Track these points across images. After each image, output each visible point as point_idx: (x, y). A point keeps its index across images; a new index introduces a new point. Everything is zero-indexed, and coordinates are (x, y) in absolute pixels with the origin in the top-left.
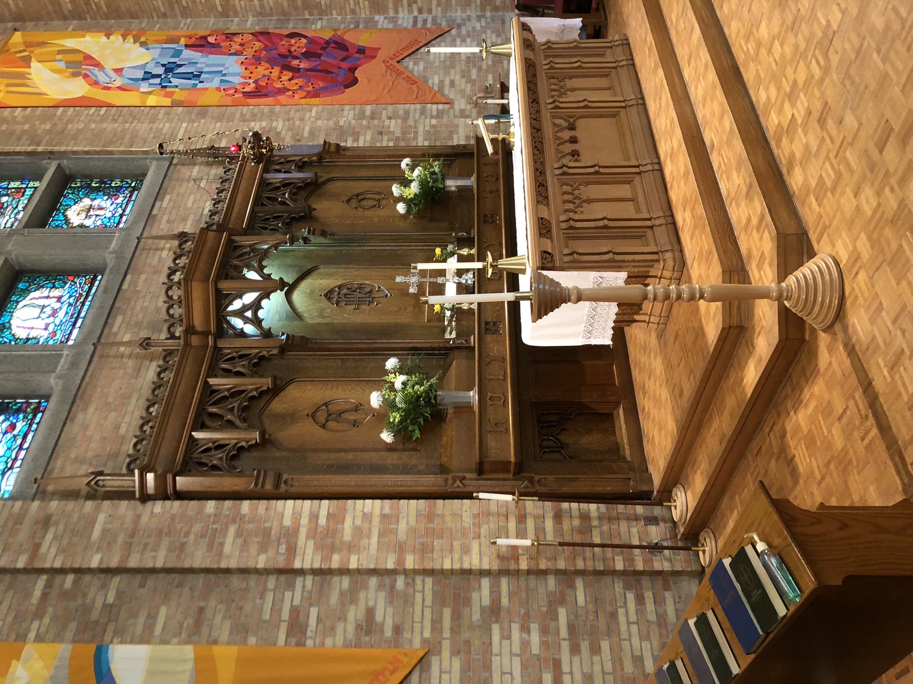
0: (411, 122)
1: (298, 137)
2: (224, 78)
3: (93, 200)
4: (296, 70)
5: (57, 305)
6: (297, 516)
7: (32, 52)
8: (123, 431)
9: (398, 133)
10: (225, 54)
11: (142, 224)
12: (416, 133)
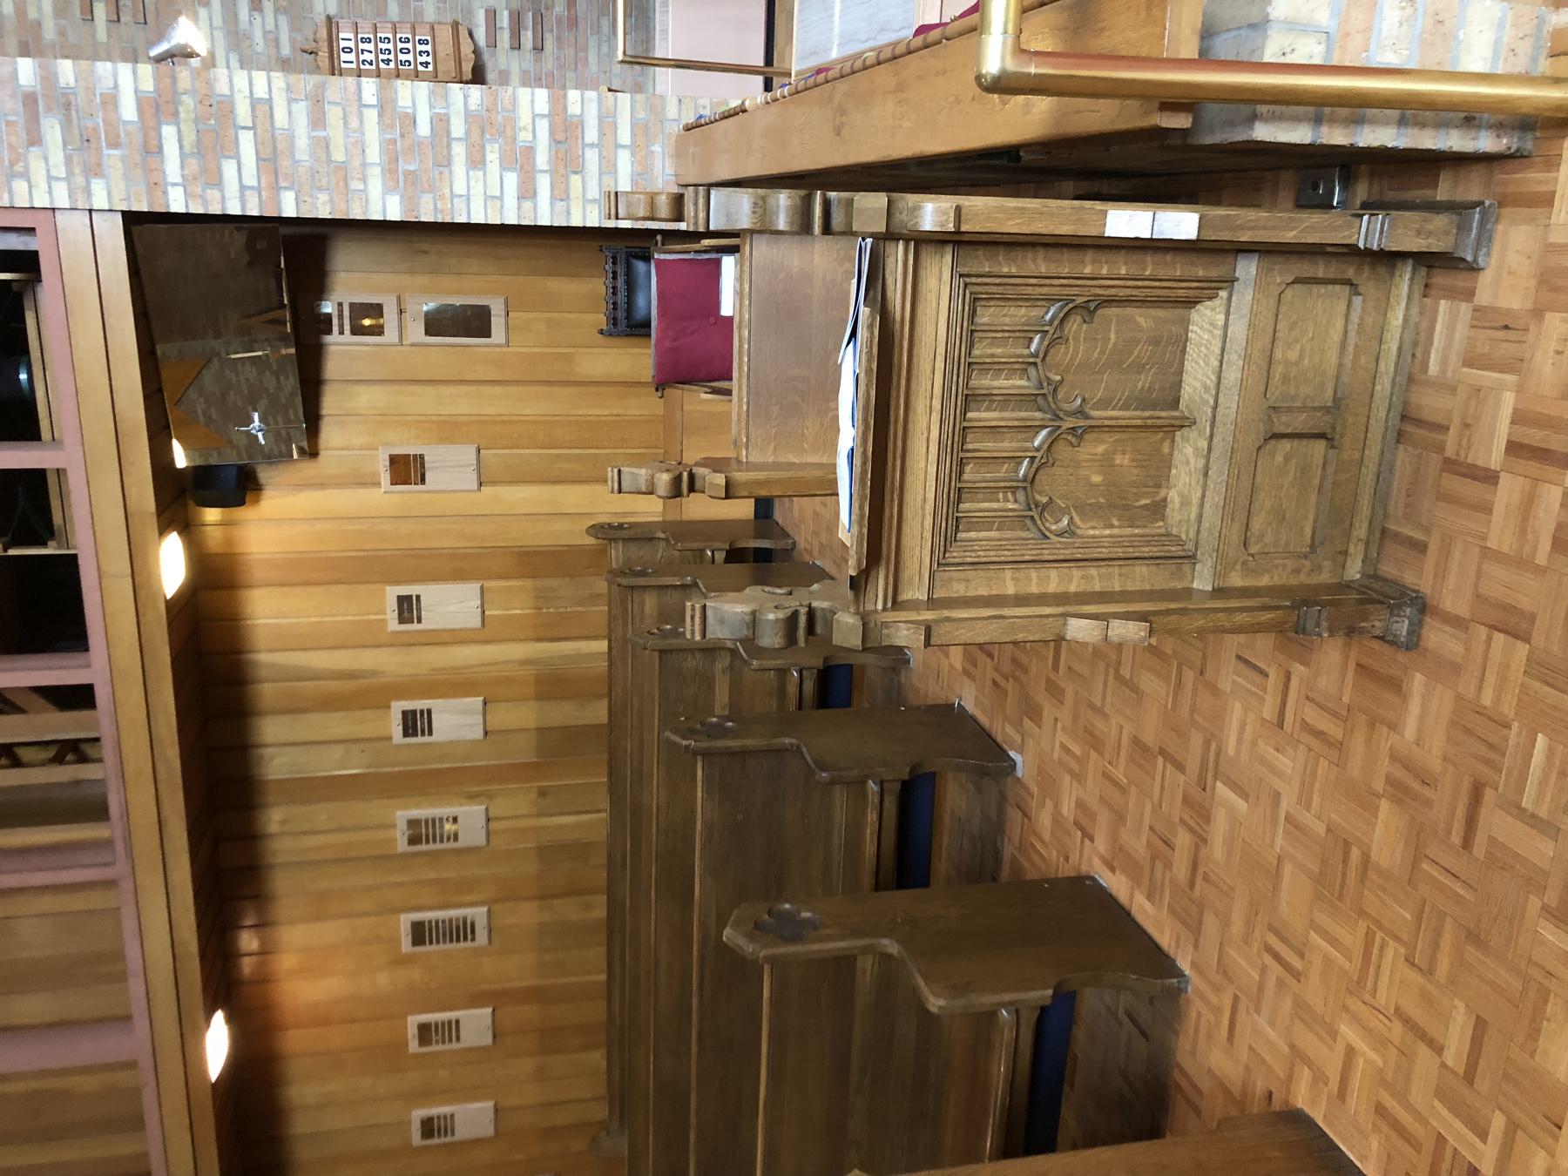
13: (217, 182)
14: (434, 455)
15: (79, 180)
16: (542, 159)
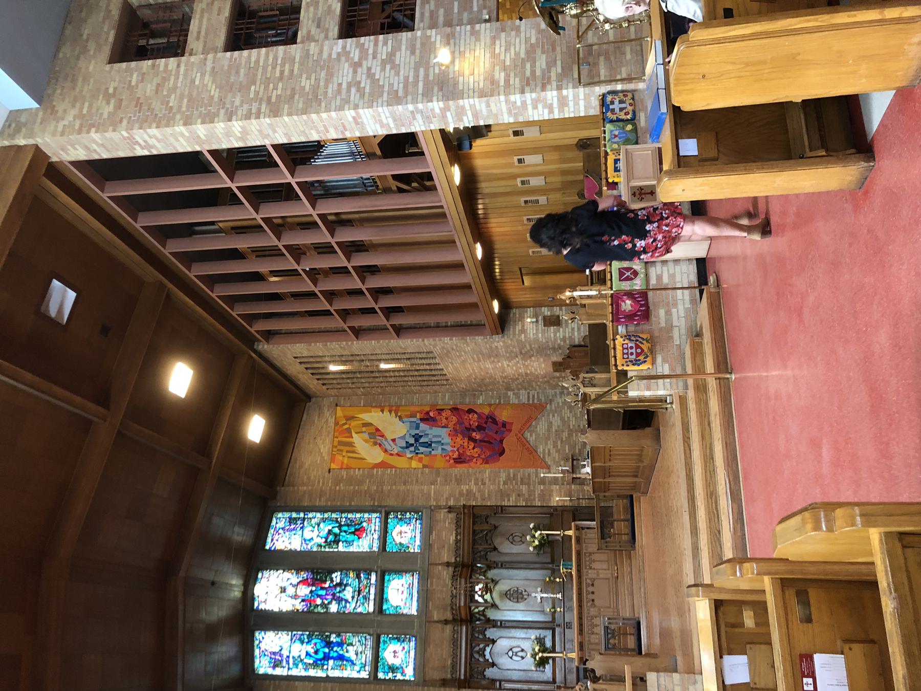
0: (532, 487)
2: (443, 447)
4: (474, 441)
7: (350, 425)
8: (444, 657)
9: (527, 496)
10: (439, 427)
12: (535, 495)
13: (462, 120)
14: (525, 130)
15: (427, 124)
16: (555, 105)
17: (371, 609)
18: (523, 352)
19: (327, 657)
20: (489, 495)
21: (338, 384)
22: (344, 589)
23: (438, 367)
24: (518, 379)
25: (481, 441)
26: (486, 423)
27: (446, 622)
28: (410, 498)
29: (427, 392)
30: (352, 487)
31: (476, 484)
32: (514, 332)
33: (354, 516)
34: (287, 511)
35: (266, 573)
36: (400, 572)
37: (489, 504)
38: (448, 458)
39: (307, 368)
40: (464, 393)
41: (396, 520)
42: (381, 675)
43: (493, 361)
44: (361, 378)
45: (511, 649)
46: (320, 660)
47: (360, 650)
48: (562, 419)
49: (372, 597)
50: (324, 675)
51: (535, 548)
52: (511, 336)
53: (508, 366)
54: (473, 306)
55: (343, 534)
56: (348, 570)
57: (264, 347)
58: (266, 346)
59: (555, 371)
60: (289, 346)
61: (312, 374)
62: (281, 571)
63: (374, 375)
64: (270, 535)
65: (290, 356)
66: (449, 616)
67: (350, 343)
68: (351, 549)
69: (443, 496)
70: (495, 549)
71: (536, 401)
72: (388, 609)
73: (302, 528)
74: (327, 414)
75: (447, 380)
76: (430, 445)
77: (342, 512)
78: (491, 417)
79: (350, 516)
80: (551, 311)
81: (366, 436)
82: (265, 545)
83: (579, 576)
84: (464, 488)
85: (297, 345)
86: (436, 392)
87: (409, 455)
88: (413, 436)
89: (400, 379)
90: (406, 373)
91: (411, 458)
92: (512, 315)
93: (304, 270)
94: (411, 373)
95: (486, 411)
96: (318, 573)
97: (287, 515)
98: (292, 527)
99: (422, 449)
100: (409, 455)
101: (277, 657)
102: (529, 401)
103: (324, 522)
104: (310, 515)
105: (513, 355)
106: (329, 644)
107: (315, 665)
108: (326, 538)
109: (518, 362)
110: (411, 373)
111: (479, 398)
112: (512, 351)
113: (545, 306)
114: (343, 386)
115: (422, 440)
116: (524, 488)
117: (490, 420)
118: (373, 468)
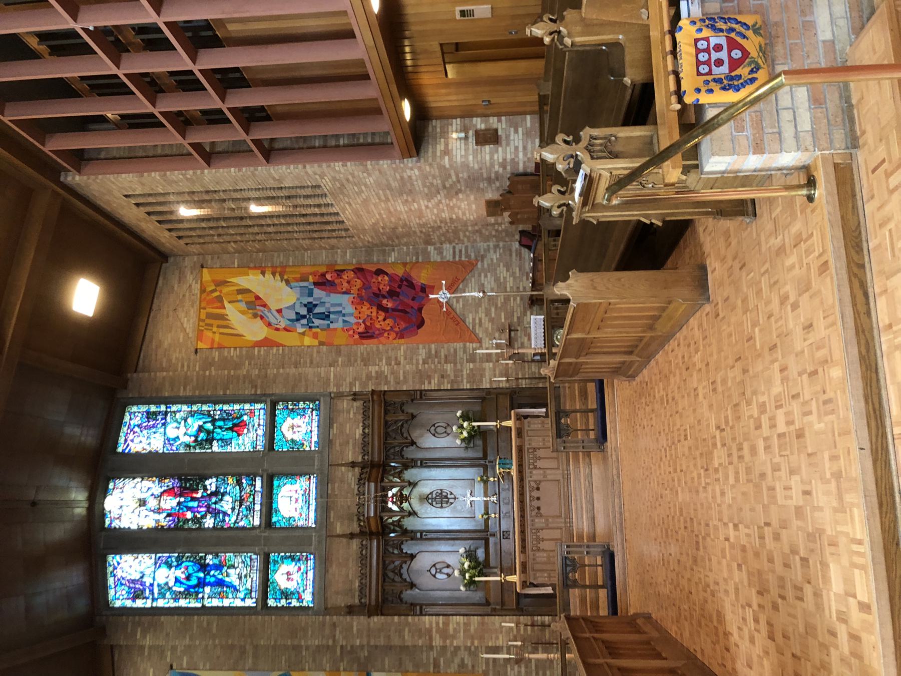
0: (459, 367)
1: (397, 380)
3: (293, 419)
4: (385, 310)
5: (296, 496)
6: (431, 623)
7: (221, 292)
9: (452, 378)
10: (340, 293)
11: (327, 449)
12: (462, 376)
17: (257, 522)
18: (448, 185)
19: (202, 583)
20: (405, 377)
21: (200, 236)
22: (221, 500)
23: (331, 210)
24: (440, 227)
25: (394, 310)
26: (400, 287)
27: (352, 536)
28: (303, 383)
29: (321, 248)
30: (226, 372)
31: (389, 364)
32: (434, 153)
33: (231, 408)
34: (143, 404)
35: (119, 483)
36: (293, 475)
37: (405, 389)
38: (351, 332)
39: (149, 214)
40: (369, 249)
41: (286, 412)
42: (271, 603)
43: (407, 201)
44: (228, 227)
45: (434, 565)
46: (194, 587)
47: (244, 572)
48: (497, 280)
49: (258, 507)
50: (199, 605)
51: (463, 440)
52: (430, 160)
53: (427, 207)
54: (371, 110)
55: (218, 430)
56: (225, 475)
57: (74, 179)
58: (77, 178)
59: (490, 214)
60: (111, 177)
61: (159, 222)
62: (139, 479)
63: (244, 223)
64: (121, 434)
65: (119, 195)
66: (356, 530)
67: (199, 172)
68: (229, 449)
69: (345, 380)
70: (413, 443)
71: (463, 258)
72: (278, 521)
73: (164, 424)
74: (190, 278)
75: (347, 230)
76: (328, 316)
77: (215, 403)
78: (407, 280)
79: (226, 407)
80: (486, 122)
81: (243, 306)
82: (116, 448)
83: (521, 479)
84: (373, 369)
85: (123, 176)
86: (333, 247)
87: (301, 330)
88: (305, 305)
89: (282, 229)
90: (289, 220)
91: (303, 334)
92: (430, 129)
93: (86, 30)
94: (296, 220)
95: (400, 272)
96: (187, 480)
97: (144, 408)
98: (151, 423)
99: (317, 322)
100: (301, 330)
101: (137, 586)
102: (454, 257)
103: (193, 416)
104: (174, 408)
105: (433, 189)
106: (204, 567)
107: (187, 594)
108: (196, 437)
109: (440, 202)
110: (296, 220)
111: (390, 255)
112: (432, 184)
113: (477, 116)
114: (207, 239)
115: (317, 310)
116: (449, 367)
117: (405, 283)
118: (253, 347)
